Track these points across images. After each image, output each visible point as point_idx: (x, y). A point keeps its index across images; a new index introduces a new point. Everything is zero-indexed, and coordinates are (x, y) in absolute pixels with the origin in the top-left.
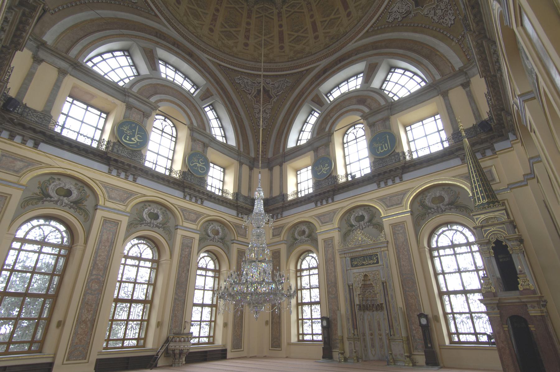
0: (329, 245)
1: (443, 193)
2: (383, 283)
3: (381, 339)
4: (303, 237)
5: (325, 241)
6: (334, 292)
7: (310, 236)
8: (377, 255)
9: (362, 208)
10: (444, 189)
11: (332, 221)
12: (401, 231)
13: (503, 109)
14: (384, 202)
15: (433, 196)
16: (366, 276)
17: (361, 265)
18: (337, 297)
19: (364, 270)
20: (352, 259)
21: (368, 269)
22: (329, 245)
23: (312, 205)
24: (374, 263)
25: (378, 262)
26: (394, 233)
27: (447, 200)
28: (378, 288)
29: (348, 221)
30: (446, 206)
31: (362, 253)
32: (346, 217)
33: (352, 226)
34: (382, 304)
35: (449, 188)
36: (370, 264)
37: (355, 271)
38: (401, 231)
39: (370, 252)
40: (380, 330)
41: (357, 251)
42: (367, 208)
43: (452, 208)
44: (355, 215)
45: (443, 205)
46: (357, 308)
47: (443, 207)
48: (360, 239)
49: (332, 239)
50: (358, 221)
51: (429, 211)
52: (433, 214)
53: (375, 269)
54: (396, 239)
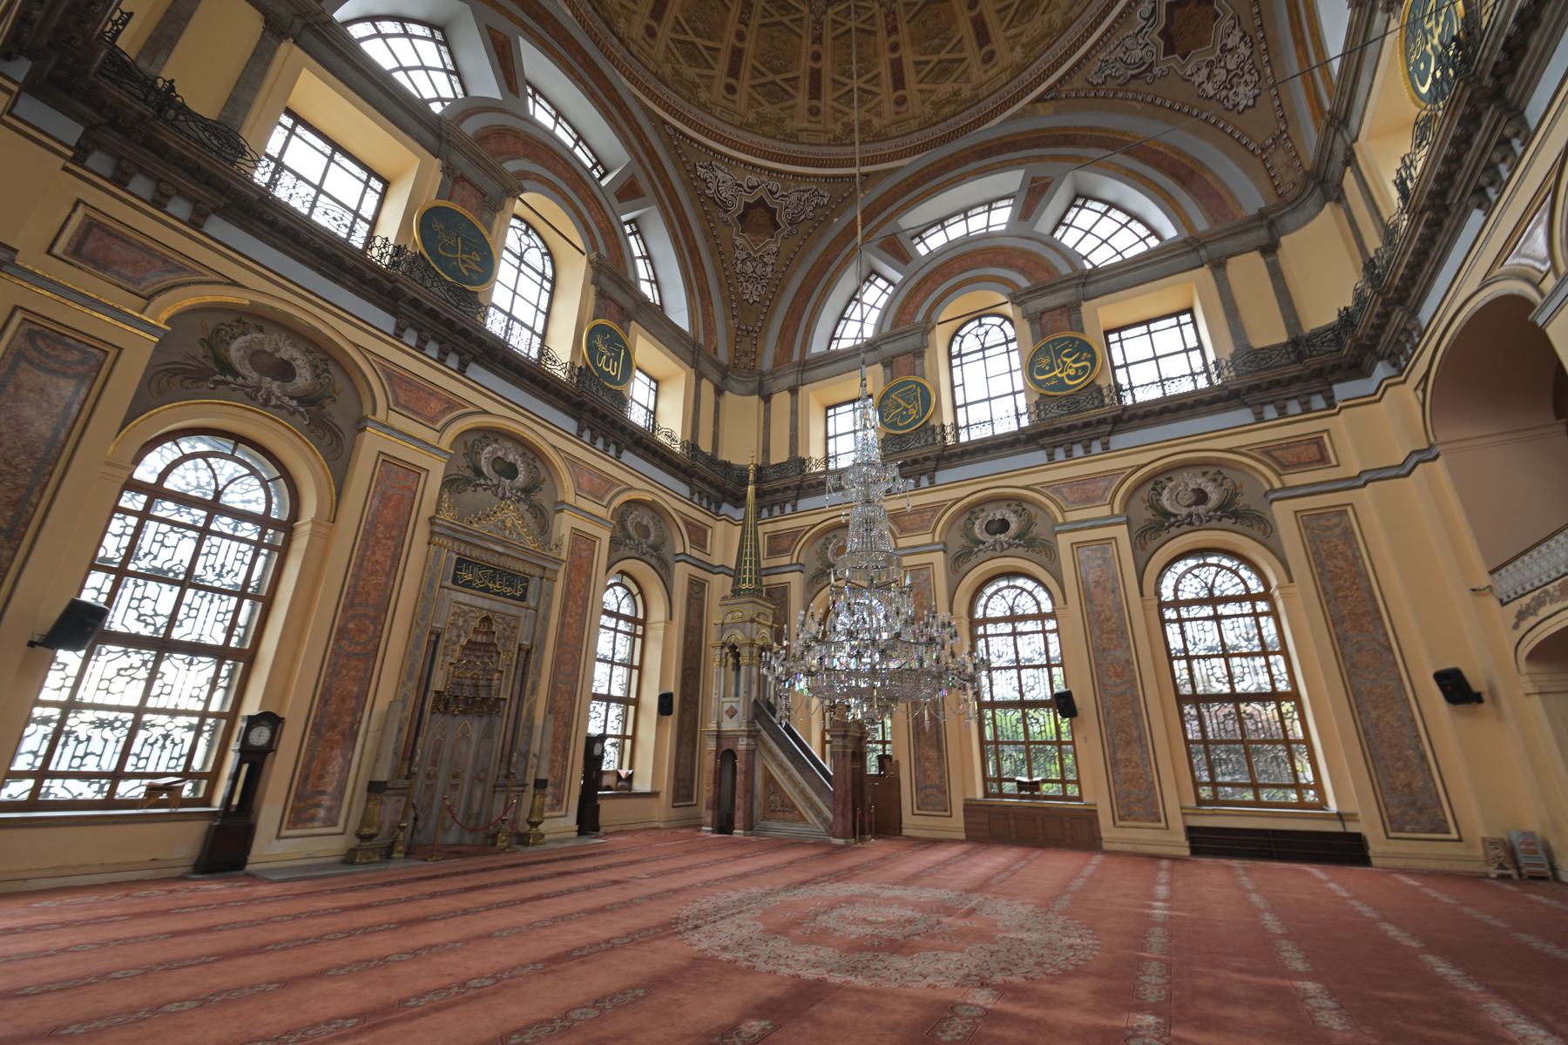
4: (275, 386)
6: (364, 637)
7: (305, 399)
8: (527, 581)
9: (521, 450)
11: (434, 420)
16: (487, 620)
17: (481, 589)
18: (370, 655)
19: (486, 604)
21: (497, 606)
23: (387, 322)
24: (513, 597)
25: (523, 598)
29: (472, 453)
31: (495, 560)
32: (470, 439)
33: (478, 472)
34: (498, 699)
36: (504, 595)
37: (461, 597)
39: (519, 566)
41: (487, 549)
42: (530, 455)
44: (495, 450)
46: (431, 696)
50: (500, 473)
53: (513, 611)
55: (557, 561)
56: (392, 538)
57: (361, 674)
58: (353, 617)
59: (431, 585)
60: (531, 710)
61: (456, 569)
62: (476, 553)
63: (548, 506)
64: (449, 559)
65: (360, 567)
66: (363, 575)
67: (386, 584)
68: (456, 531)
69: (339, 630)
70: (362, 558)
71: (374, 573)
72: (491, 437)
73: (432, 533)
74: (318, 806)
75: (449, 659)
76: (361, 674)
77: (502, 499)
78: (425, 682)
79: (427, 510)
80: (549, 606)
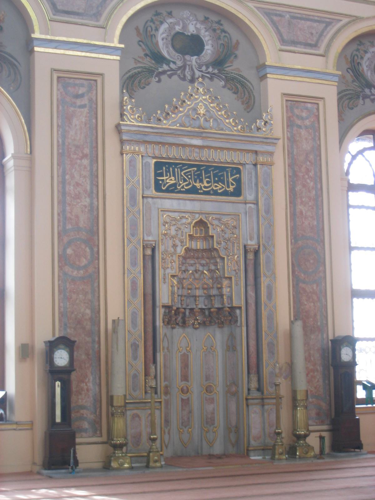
0: (77, 96)
2: (246, 252)
3: (186, 402)
5: (64, 79)
6: (84, 262)
8: (239, 171)
9: (201, 15)
11: (97, 15)
12: (307, 122)
14: (274, 24)
16: (201, 224)
17: (188, 192)
18: (93, 279)
20: (161, 167)
22: (77, 96)
24: (225, 193)
25: (237, 192)
26: (290, 124)
28: (233, 264)
31: (195, 155)
32: (140, 23)
33: (159, 58)
36: (216, 193)
38: (307, 122)
40: (185, 378)
41: (184, 146)
42: (214, 18)
44: (171, 27)
48: (202, 111)
49: (92, 80)
50: (183, 51)
51: (367, 91)
53: (228, 208)
54: (292, 140)
55: (272, 141)
56: (85, 156)
57: (90, 296)
58: (69, 243)
59: (133, 198)
60: (271, 318)
61: (157, 175)
62: (174, 153)
63: (250, 75)
64: (145, 166)
65: (63, 193)
66: (68, 199)
67: (91, 204)
68: (146, 134)
69: (60, 257)
70: (63, 183)
71: (78, 197)
72: (163, 11)
73: (122, 142)
74: (82, 418)
75: (169, 272)
76: (90, 296)
77: (192, 81)
78: (151, 297)
79: (111, 118)
80: (270, 196)
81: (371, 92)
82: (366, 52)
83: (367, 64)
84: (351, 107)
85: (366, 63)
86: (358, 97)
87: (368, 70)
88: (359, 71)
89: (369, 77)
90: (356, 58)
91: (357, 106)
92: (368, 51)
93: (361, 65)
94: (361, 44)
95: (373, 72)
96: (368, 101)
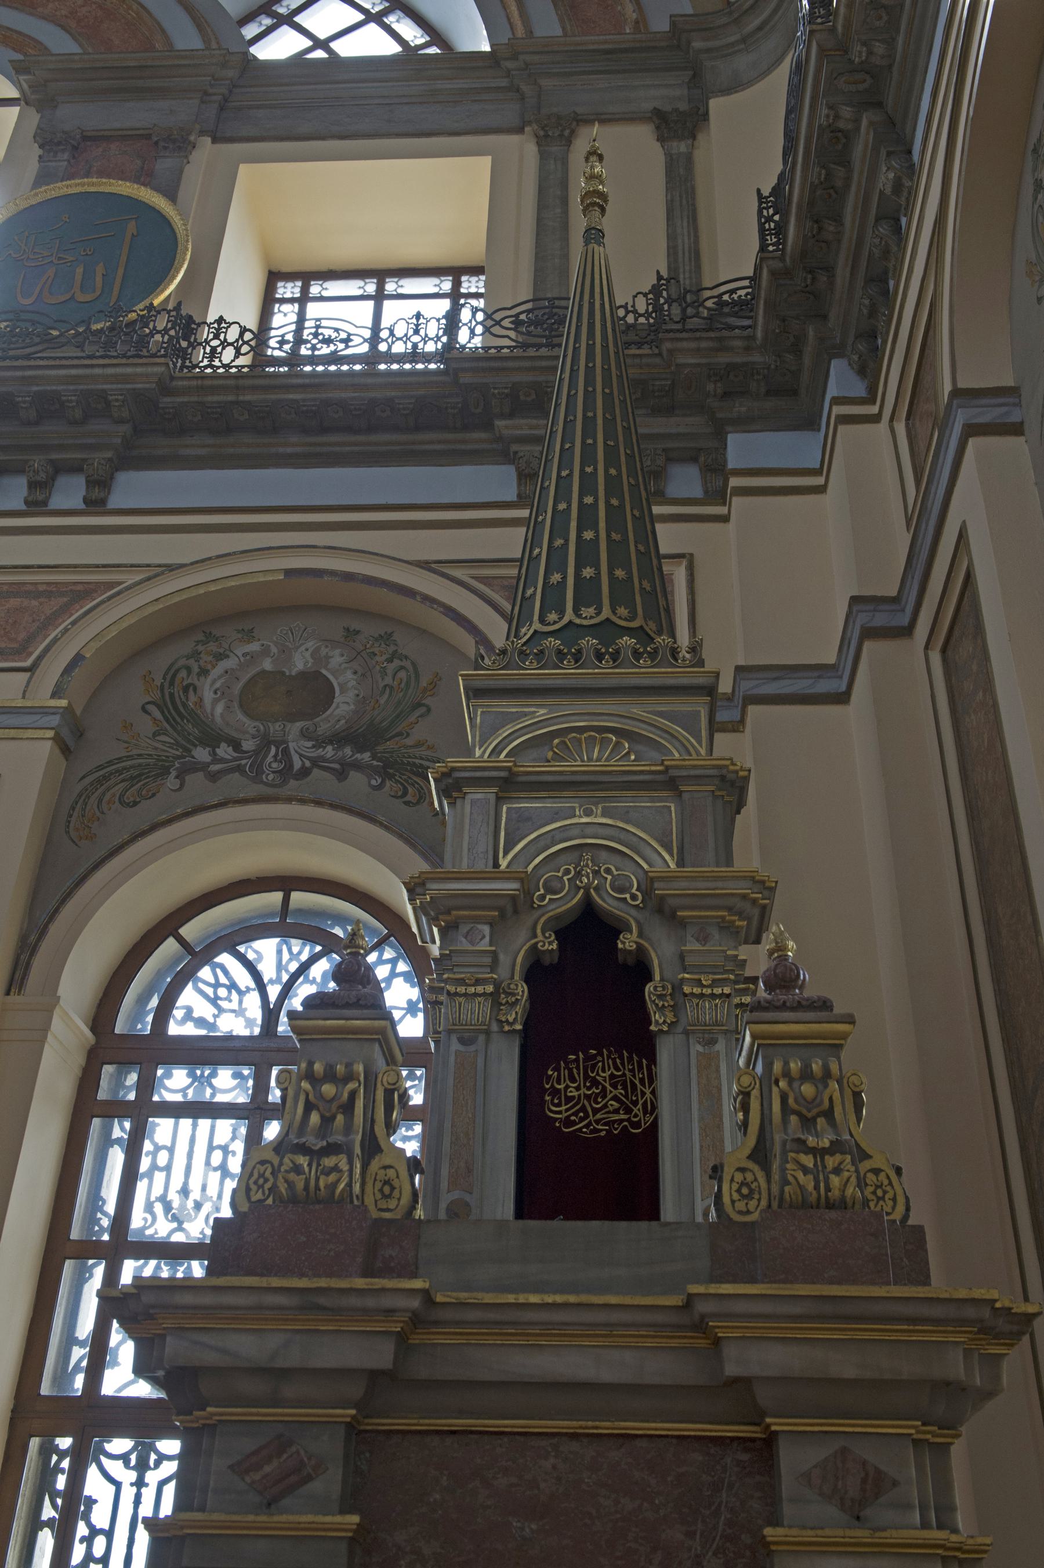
1: (337, 658)
10: (351, 634)
13: (872, 101)
15: (267, 665)
27: (343, 706)
30: (320, 742)
35: (387, 638)
43: (357, 766)
45: (305, 734)
47: (300, 750)
51: (202, 754)
52: (214, 777)
81: (214, 754)
82: (220, 657)
83: (218, 685)
84: (132, 799)
85: (214, 681)
86: (165, 772)
87: (215, 702)
88: (184, 705)
89: (218, 720)
90: (183, 673)
91: (154, 795)
92: (228, 652)
93: (195, 690)
94: (209, 637)
95: (236, 704)
96: (197, 780)
